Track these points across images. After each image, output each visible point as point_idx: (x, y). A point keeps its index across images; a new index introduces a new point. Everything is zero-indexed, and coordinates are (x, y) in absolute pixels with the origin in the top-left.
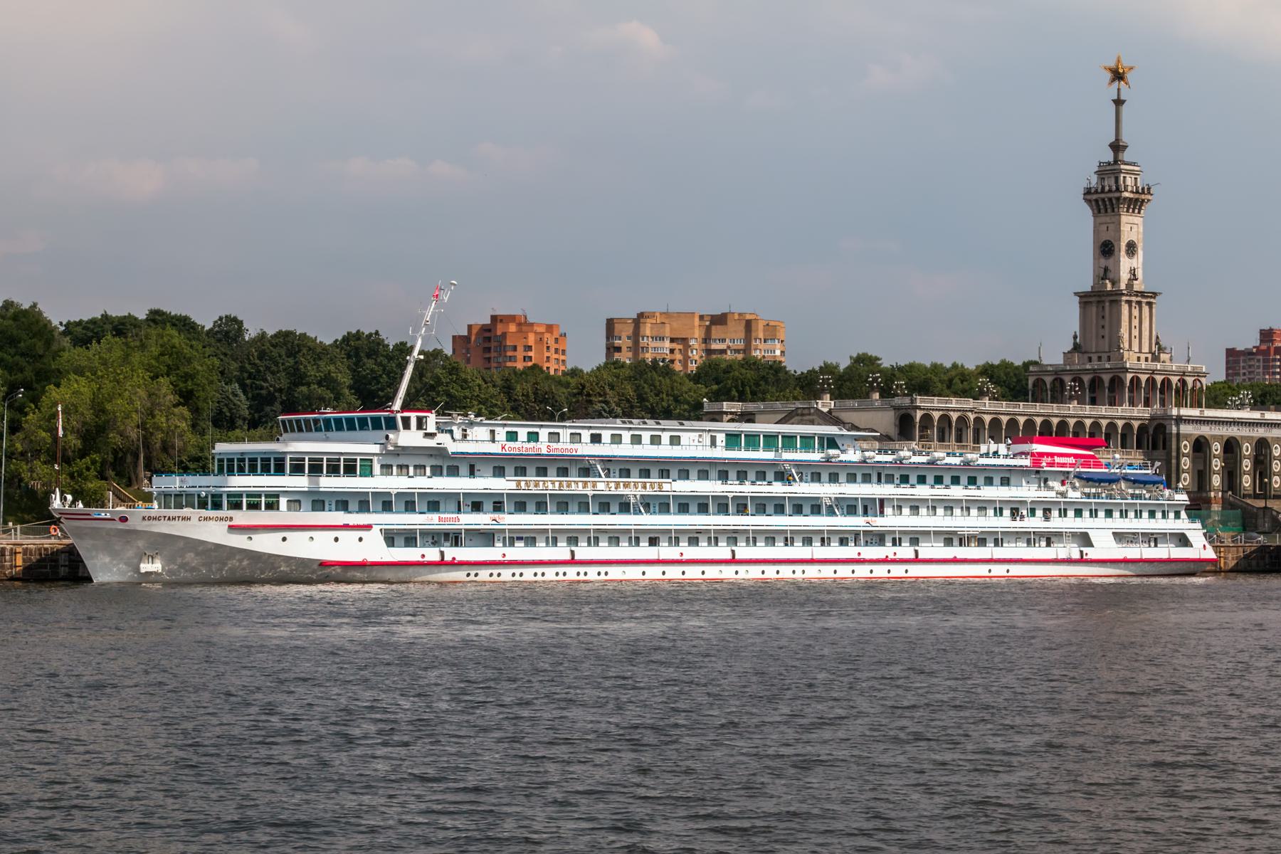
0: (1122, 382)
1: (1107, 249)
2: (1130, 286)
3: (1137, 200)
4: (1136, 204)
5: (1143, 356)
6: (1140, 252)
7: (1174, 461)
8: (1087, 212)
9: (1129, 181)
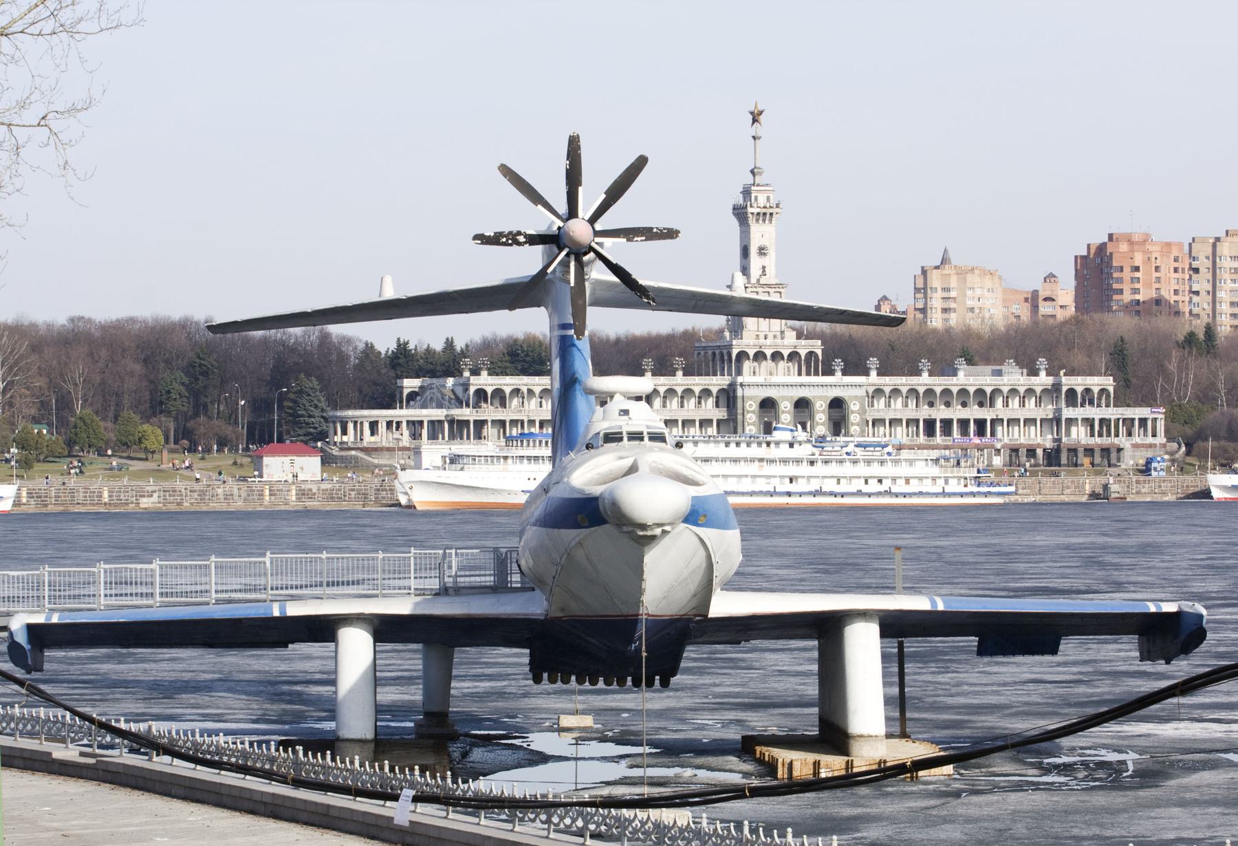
0: (730, 355)
1: (745, 252)
2: (758, 281)
3: (765, 214)
4: (763, 216)
5: (770, 335)
6: (772, 253)
7: (740, 417)
8: (735, 222)
9: (762, 200)
